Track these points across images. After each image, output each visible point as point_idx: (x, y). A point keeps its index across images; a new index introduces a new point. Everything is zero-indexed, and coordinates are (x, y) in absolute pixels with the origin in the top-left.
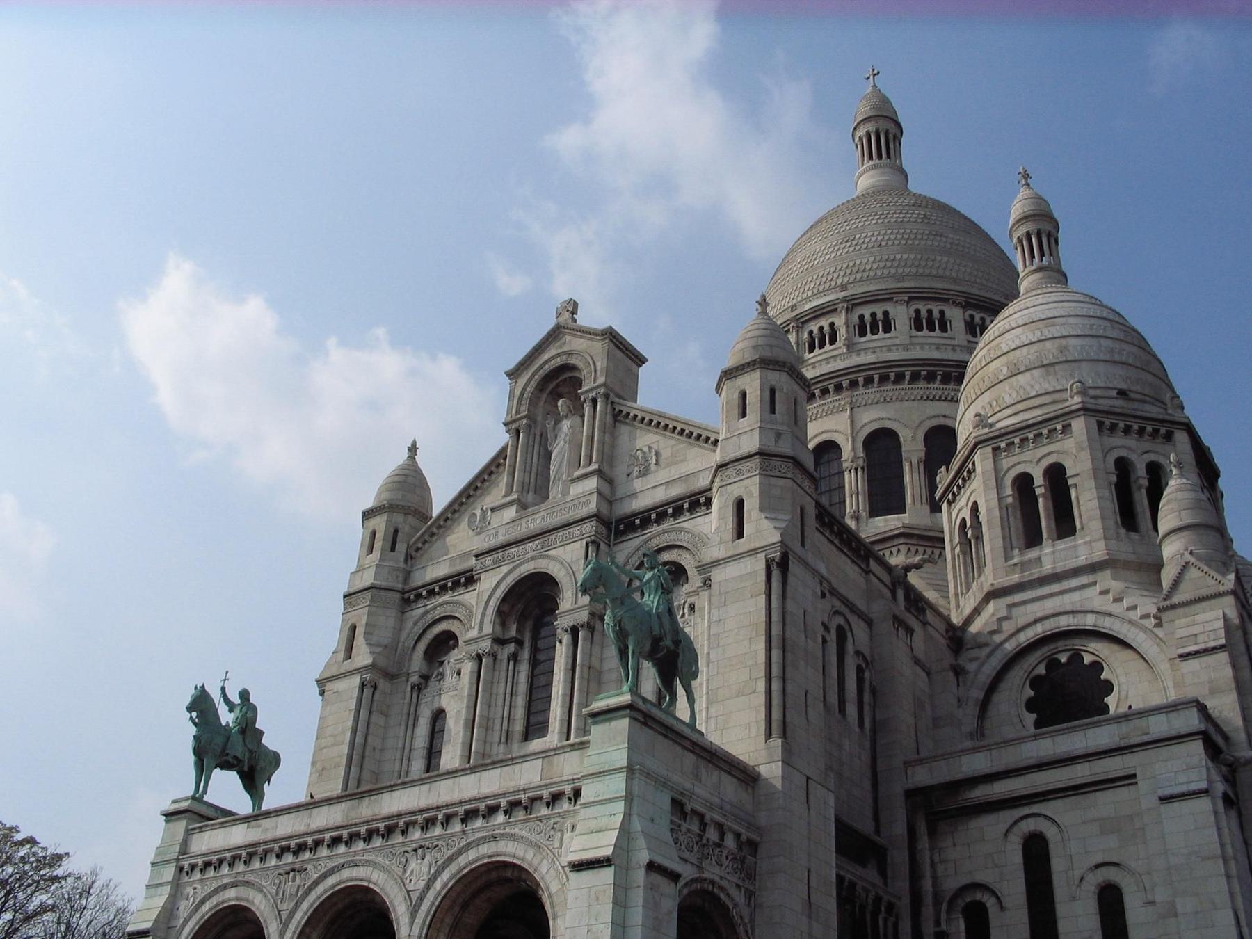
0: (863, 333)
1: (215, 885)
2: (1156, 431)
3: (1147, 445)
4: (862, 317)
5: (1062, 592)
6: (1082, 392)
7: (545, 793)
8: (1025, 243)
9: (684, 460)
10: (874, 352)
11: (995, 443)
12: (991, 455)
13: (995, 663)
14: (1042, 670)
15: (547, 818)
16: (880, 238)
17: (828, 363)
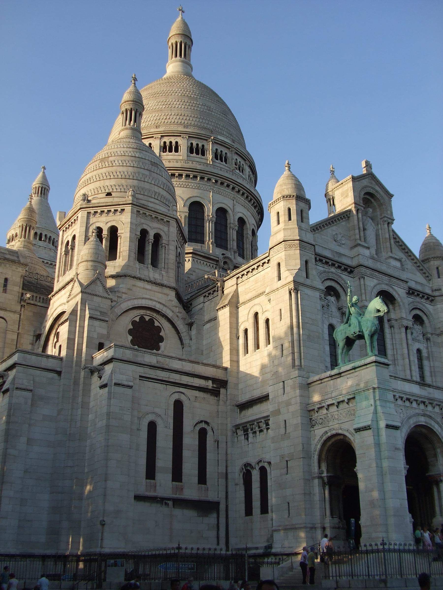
4: (236, 159)
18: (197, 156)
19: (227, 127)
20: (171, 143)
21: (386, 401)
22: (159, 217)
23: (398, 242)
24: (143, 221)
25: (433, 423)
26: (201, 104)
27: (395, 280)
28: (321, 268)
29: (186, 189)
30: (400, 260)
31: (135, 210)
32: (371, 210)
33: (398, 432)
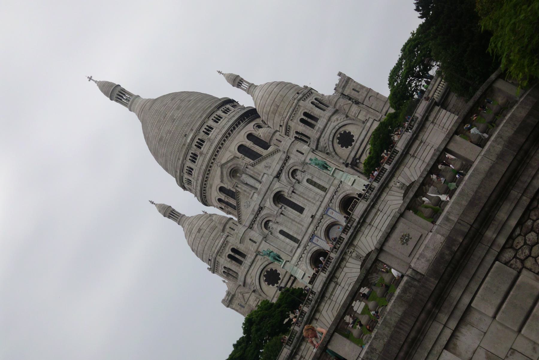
0: (208, 134)
1: (305, 259)
2: (309, 94)
3: (311, 98)
4: (204, 131)
5: (328, 128)
6: (295, 99)
7: (338, 187)
8: (240, 85)
9: (275, 158)
10: (219, 134)
11: (290, 119)
12: (292, 122)
13: (331, 147)
14: (338, 141)
15: (341, 189)
16: (181, 113)
17: (212, 146)
18: (197, 160)
19: (182, 126)
20: (187, 169)
21: (296, 272)
22: (224, 245)
23: (257, 162)
24: (224, 255)
25: (313, 250)
26: (165, 136)
27: (271, 186)
28: (255, 226)
29: (215, 178)
30: (264, 173)
31: (218, 257)
32: (238, 175)
33: (306, 274)
